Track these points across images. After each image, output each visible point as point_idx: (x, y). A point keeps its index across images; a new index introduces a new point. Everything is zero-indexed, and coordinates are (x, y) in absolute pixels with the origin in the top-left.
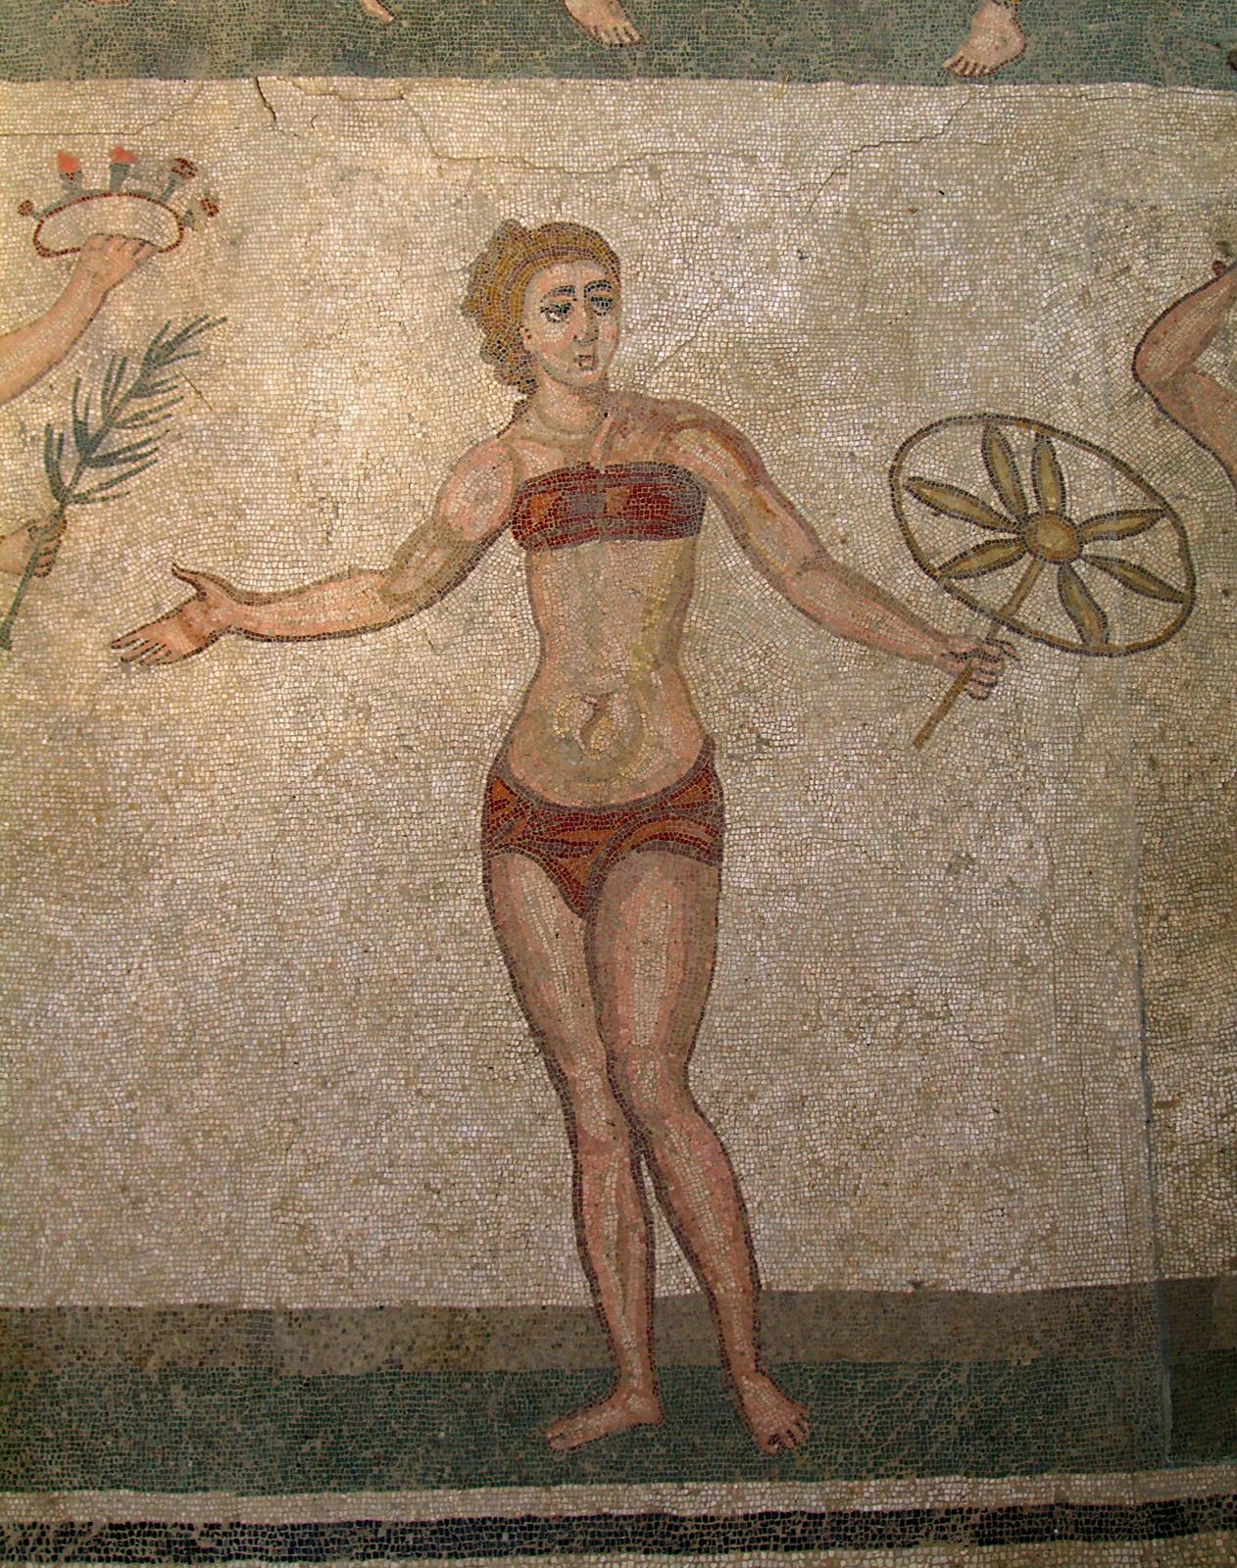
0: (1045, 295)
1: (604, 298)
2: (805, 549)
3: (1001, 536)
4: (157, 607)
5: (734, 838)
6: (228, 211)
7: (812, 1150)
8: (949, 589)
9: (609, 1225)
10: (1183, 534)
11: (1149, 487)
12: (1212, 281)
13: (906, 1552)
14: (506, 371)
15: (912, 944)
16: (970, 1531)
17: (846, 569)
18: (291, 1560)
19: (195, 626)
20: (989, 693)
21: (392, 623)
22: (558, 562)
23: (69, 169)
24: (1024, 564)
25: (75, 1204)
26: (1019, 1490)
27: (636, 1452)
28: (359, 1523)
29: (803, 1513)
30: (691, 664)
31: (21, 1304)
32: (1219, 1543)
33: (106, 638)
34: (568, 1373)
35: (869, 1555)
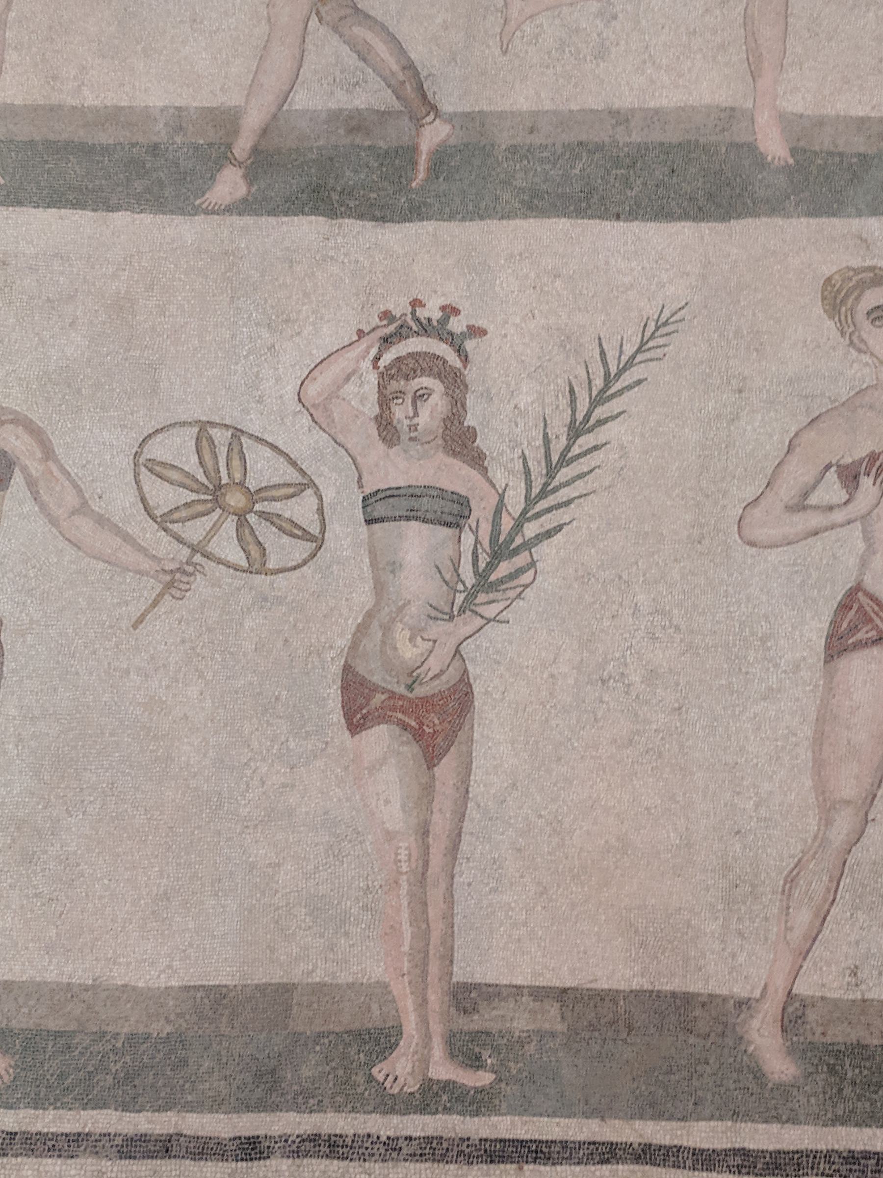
0: (246, 348)
3: (202, 497)
10: (321, 499)
11: (301, 469)
12: (357, 341)
15: (117, 755)
20: (184, 596)
24: (215, 515)
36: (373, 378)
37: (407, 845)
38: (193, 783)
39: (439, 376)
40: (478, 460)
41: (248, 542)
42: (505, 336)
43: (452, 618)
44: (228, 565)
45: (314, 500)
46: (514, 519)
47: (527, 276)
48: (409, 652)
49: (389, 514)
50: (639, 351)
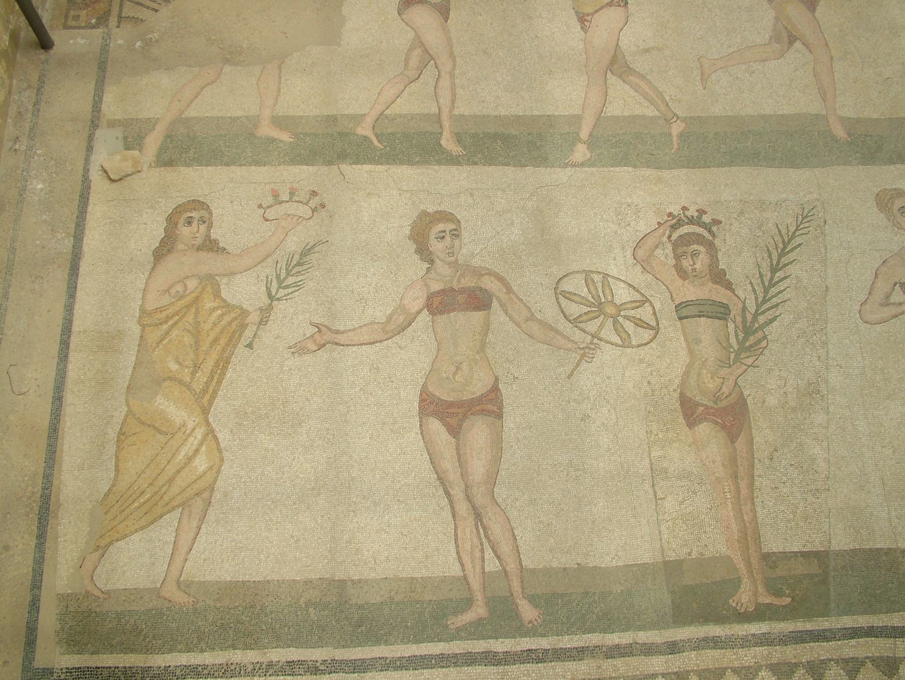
1: (456, 234)
3: (593, 309)
4: (304, 335)
5: (507, 410)
7: (539, 518)
8: (576, 327)
9: (468, 546)
10: (654, 308)
13: (580, 662)
14: (424, 258)
16: (603, 654)
17: (541, 320)
18: (354, 673)
19: (318, 341)
22: (442, 319)
23: (276, 195)
25: (274, 542)
26: (620, 638)
27: (480, 628)
28: (379, 658)
29: (542, 649)
30: (489, 352)
31: (254, 579)
32: (693, 656)
33: (287, 345)
34: (455, 600)
35: (567, 664)
36: (669, 246)
40: (729, 286)
41: (620, 332)
43: (730, 366)
45: (650, 309)
46: (752, 314)
48: (711, 386)
50: (796, 230)
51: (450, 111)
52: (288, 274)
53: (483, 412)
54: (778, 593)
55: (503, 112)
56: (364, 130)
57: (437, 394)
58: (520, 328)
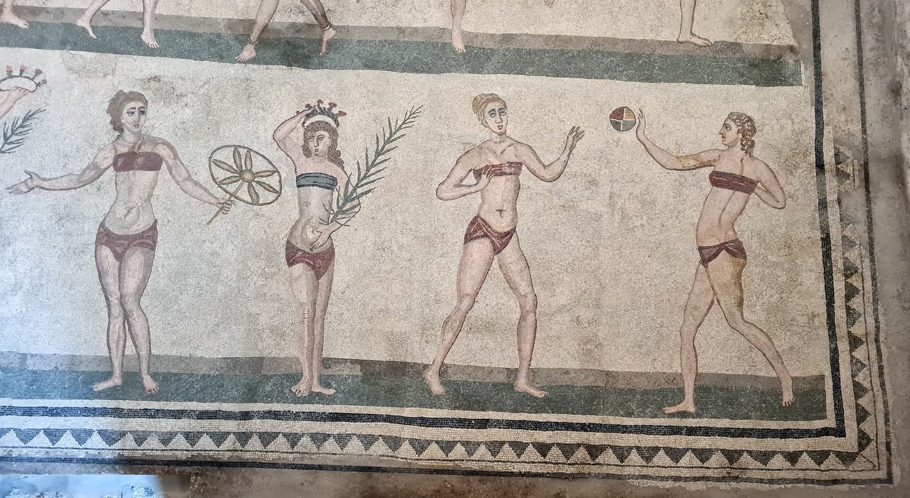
2: (187, 176)
4: (20, 180)
6: (49, 83)
9: (116, 336)
13: (179, 420)
21: (79, 187)
22: (124, 174)
33: (6, 187)
36: (302, 130)
37: (308, 307)
38: (229, 284)
39: (327, 131)
40: (341, 164)
42: (353, 116)
43: (328, 224)
44: (244, 201)
47: (363, 92)
48: (311, 236)
49: (306, 183)
50: (403, 123)
51: (153, 12)
52: (13, 133)
53: (142, 245)
54: (328, 386)
55: (194, 14)
56: (83, 22)
57: (111, 229)
58: (179, 185)
